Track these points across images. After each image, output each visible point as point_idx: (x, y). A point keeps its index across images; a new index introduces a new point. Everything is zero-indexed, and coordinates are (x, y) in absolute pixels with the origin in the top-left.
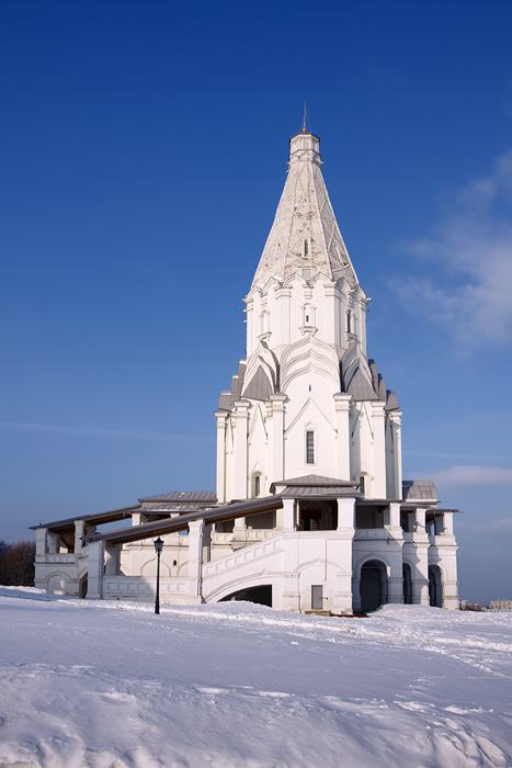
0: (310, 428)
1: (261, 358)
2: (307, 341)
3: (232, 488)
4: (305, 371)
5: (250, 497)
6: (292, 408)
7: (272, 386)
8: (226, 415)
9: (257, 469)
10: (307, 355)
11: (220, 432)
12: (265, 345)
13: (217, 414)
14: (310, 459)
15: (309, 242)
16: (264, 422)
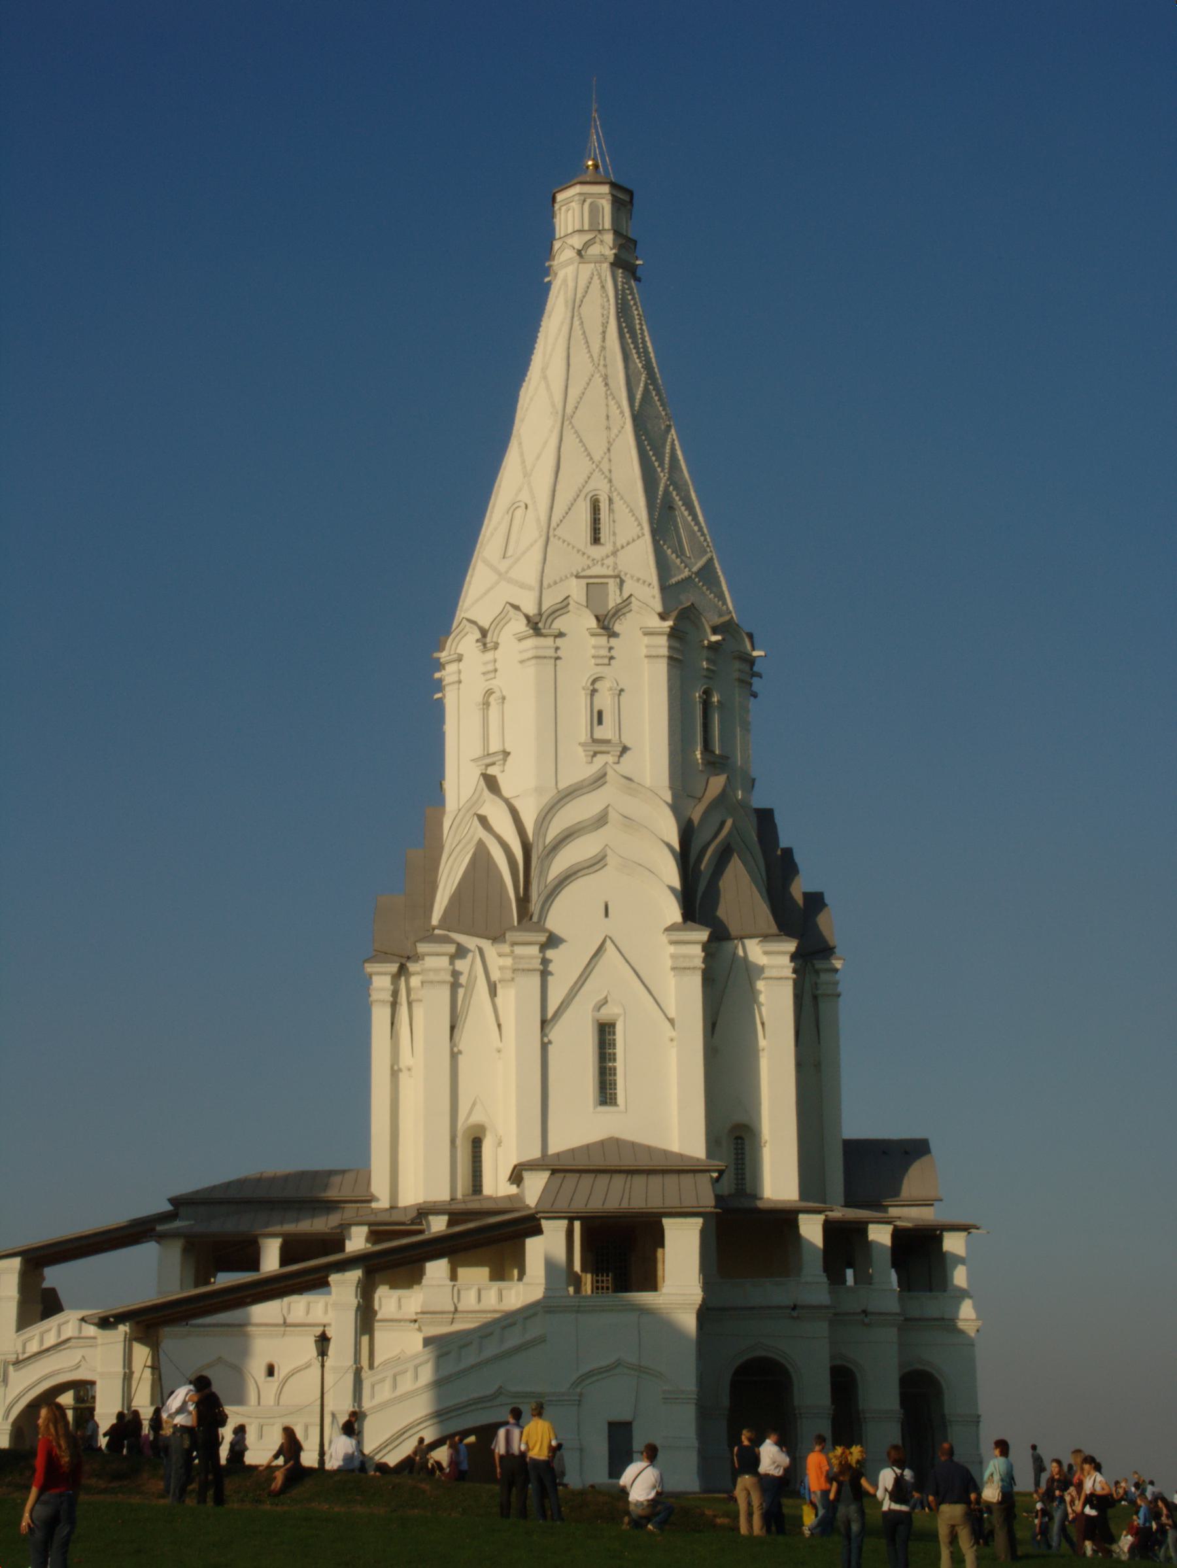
0: (606, 1014)
1: (483, 820)
2: (599, 780)
3: (411, 1173)
4: (597, 863)
5: (459, 1196)
6: (566, 964)
7: (516, 902)
8: (394, 968)
9: (476, 1118)
10: (601, 820)
11: (380, 1016)
12: (491, 783)
13: (370, 968)
14: (606, 1092)
15: (604, 506)
16: (493, 990)
